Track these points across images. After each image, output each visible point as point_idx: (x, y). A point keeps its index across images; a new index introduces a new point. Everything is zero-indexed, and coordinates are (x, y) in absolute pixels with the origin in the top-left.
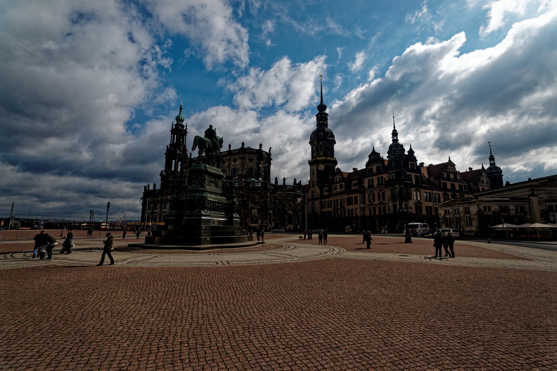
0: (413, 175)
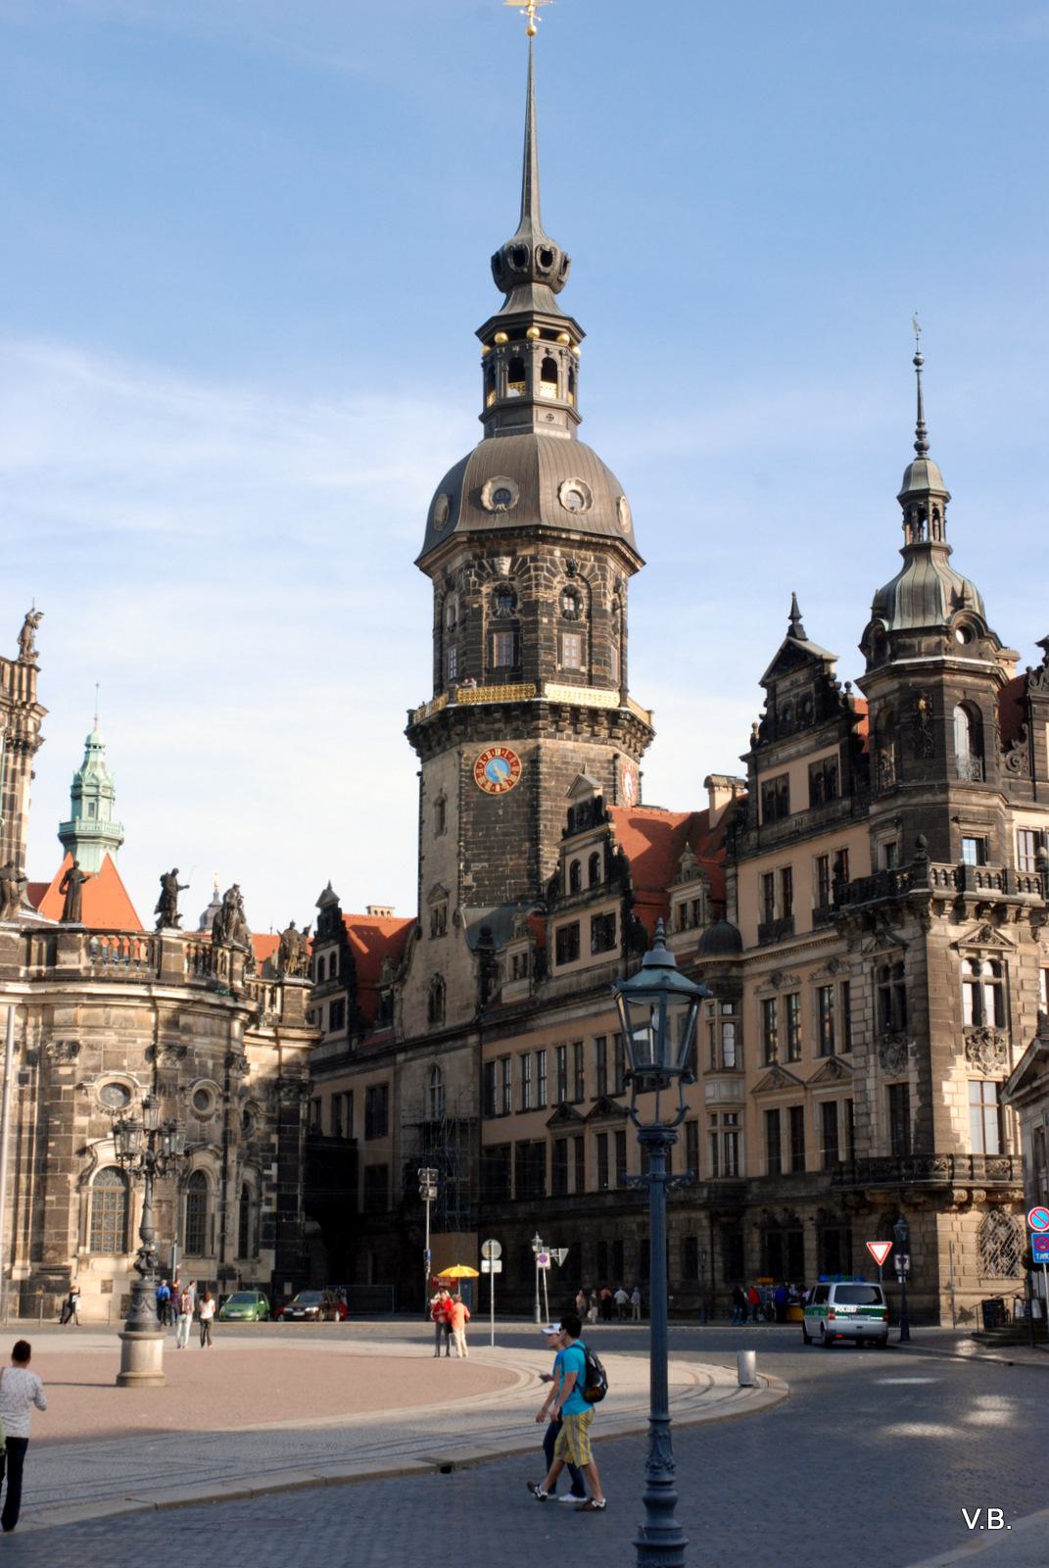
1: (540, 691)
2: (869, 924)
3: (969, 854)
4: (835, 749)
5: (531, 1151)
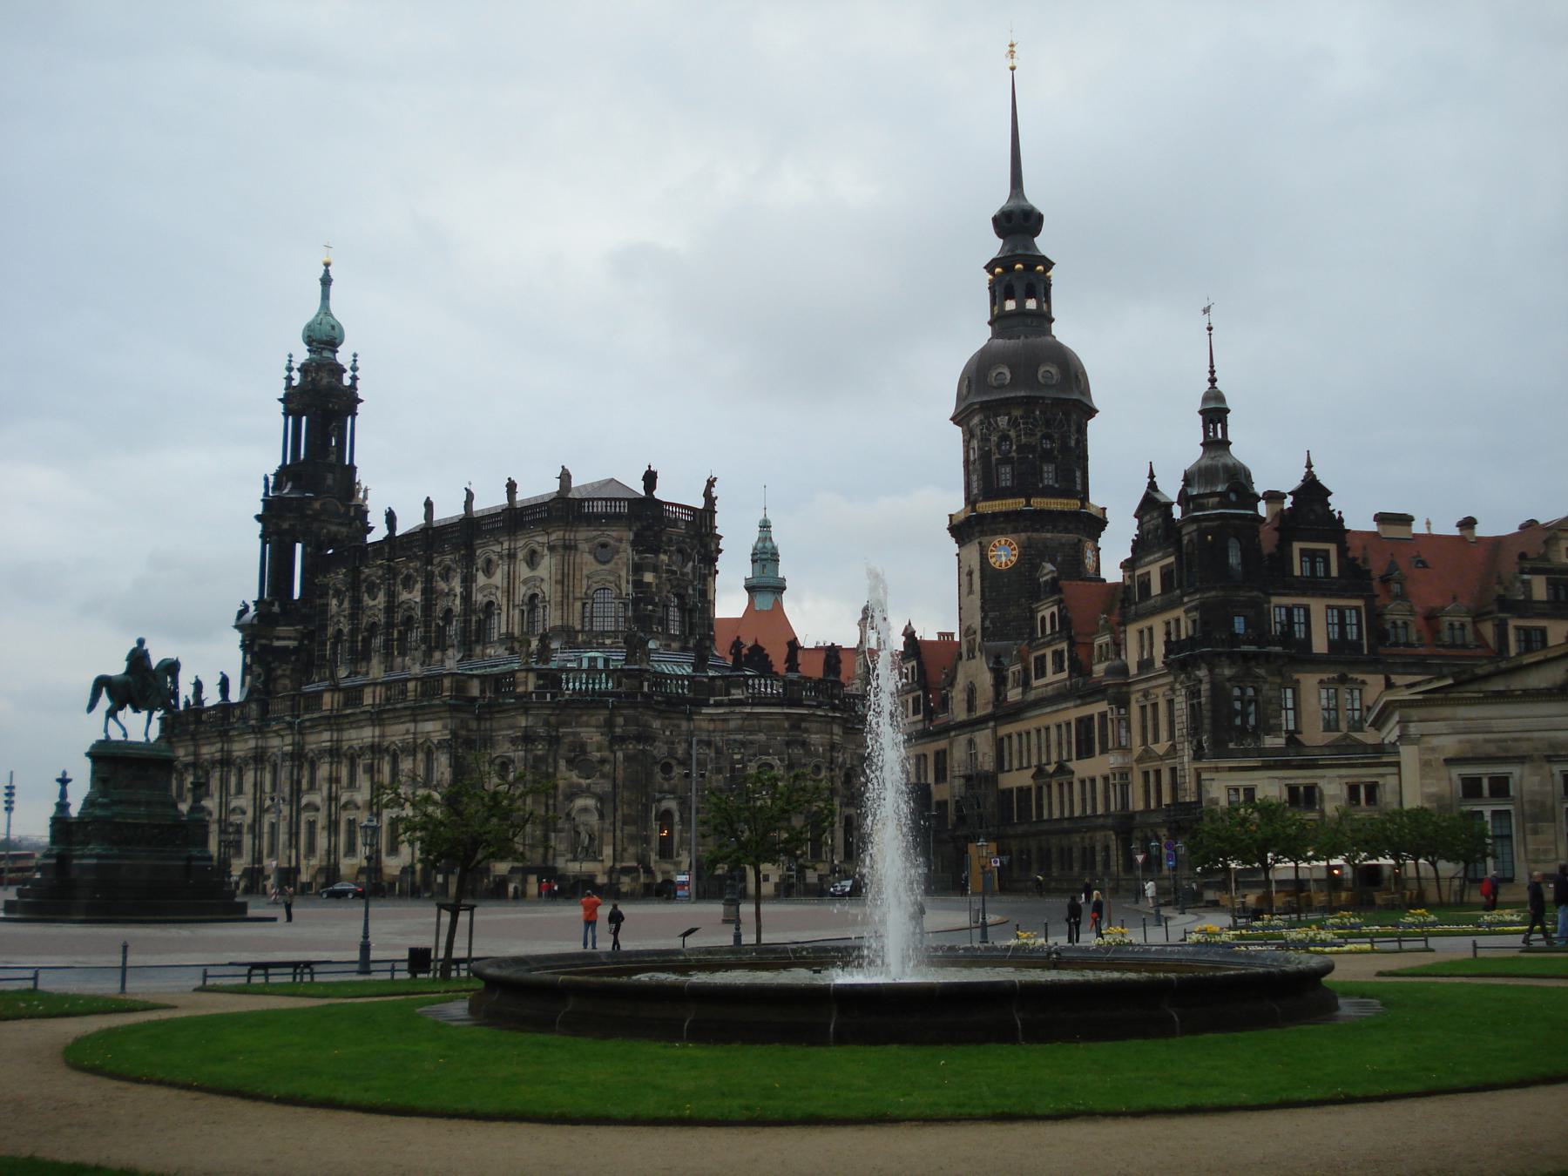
0: (1318, 606)
1: (1028, 504)
3: (1239, 625)
5: (1024, 792)
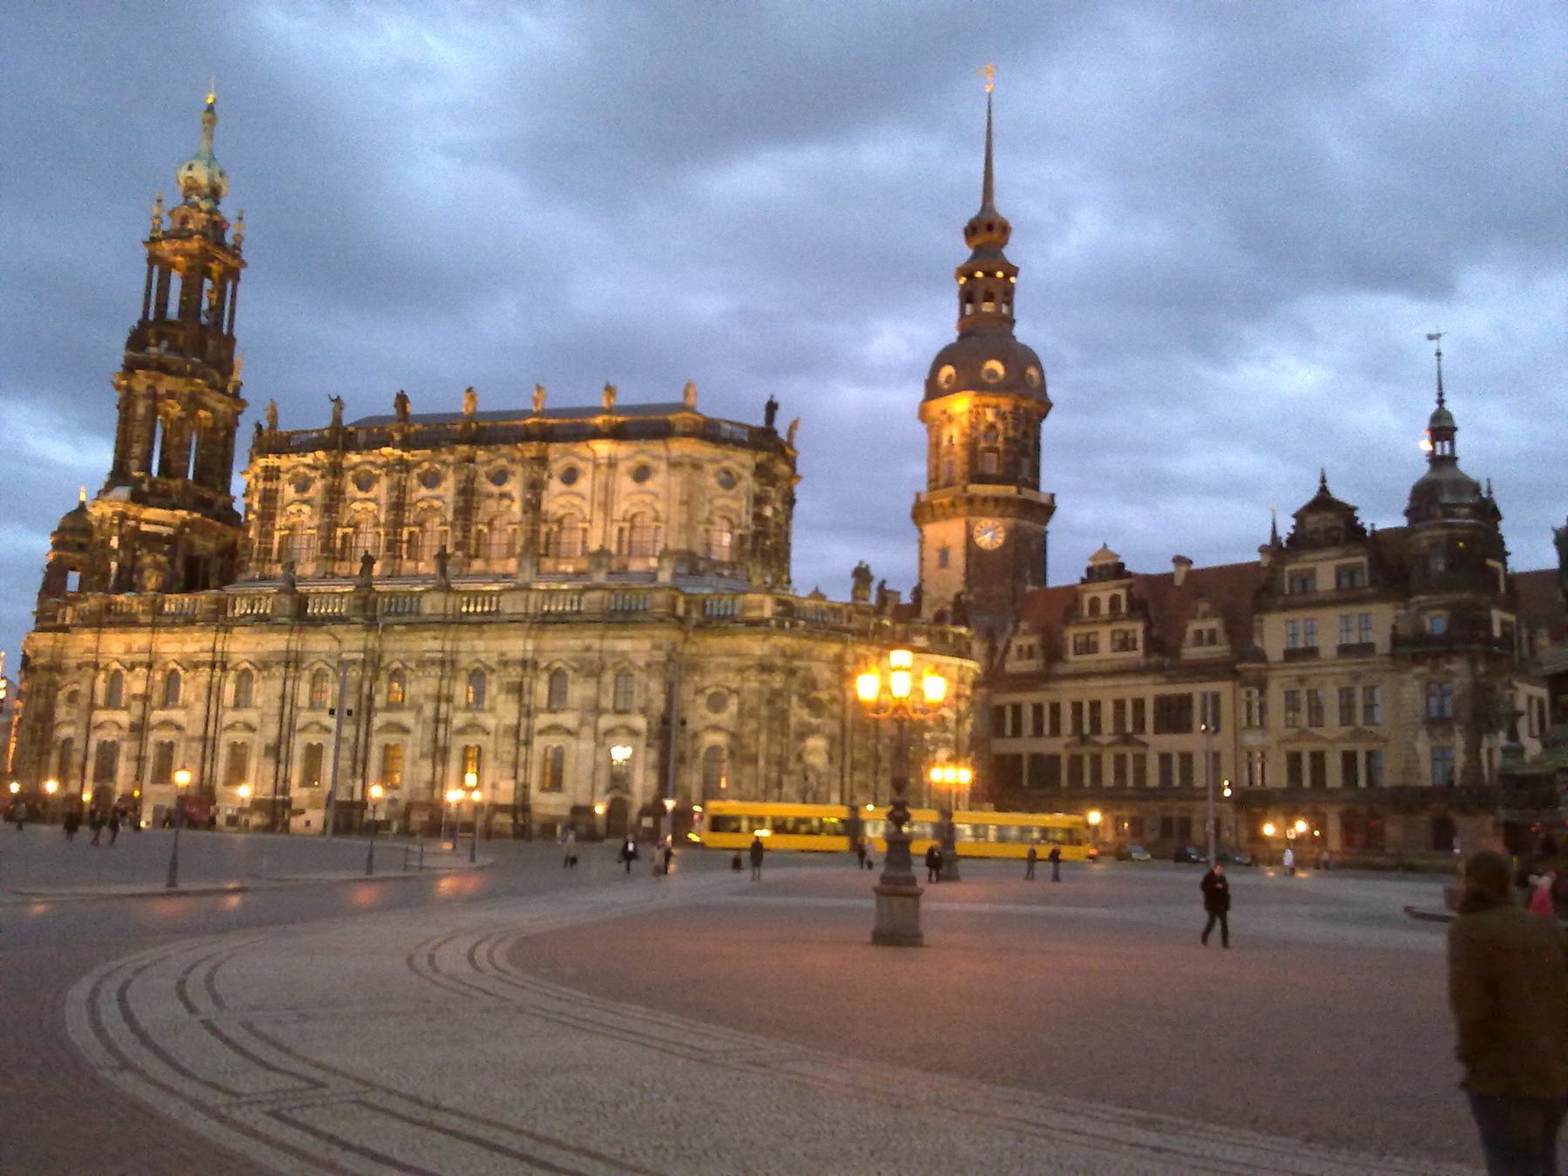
0: (1497, 616)
2: (1417, 659)
4: (1363, 559)
